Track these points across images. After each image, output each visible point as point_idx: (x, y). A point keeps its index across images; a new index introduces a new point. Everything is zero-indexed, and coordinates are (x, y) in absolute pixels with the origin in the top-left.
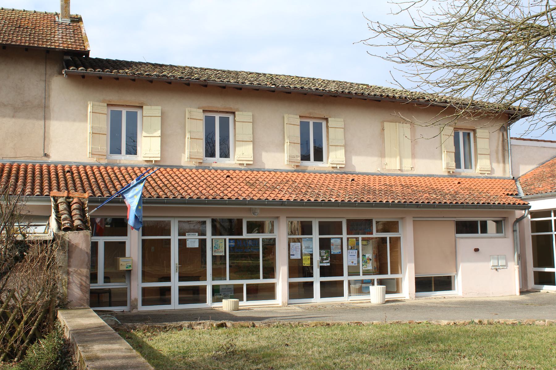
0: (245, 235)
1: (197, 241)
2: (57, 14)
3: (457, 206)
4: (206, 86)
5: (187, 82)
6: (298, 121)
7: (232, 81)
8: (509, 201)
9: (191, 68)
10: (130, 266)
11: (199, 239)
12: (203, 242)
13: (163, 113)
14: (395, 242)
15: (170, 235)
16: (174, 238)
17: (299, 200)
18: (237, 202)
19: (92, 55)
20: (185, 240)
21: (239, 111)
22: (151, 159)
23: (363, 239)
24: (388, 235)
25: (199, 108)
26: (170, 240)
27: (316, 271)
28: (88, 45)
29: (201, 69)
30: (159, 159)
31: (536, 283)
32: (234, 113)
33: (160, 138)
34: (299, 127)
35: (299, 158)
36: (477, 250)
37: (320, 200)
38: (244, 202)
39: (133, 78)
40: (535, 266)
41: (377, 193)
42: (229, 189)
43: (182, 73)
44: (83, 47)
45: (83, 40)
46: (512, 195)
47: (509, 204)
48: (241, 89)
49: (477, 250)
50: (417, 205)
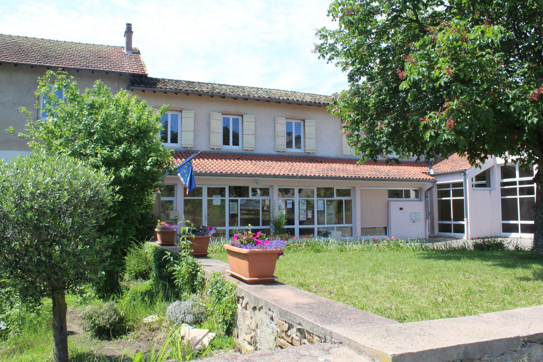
0: (251, 197)
1: (220, 201)
2: (122, 47)
3: (389, 180)
4: (224, 98)
5: (212, 95)
6: (284, 121)
7: (241, 94)
8: (423, 177)
9: (212, 84)
10: (177, 216)
11: (221, 200)
12: (223, 201)
13: (195, 115)
14: (348, 203)
15: (202, 196)
16: (205, 198)
17: (291, 175)
18: (246, 175)
19: (148, 76)
20: (212, 200)
21: (245, 114)
22: (187, 146)
23: (328, 201)
24: (344, 199)
25: (219, 112)
26: (202, 200)
27: (297, 222)
28: (146, 70)
29: (219, 85)
30: (192, 146)
31: (440, 231)
32: (242, 116)
33: (193, 132)
34: (285, 126)
35: (286, 147)
36: (401, 209)
37: (300, 175)
38: (251, 175)
39: (176, 92)
40: (439, 220)
41: (337, 170)
42: (240, 167)
43: (208, 88)
44: (143, 71)
45: (142, 66)
46: (425, 173)
47: (423, 179)
48: (247, 100)
49: (401, 209)
50: (363, 179)
